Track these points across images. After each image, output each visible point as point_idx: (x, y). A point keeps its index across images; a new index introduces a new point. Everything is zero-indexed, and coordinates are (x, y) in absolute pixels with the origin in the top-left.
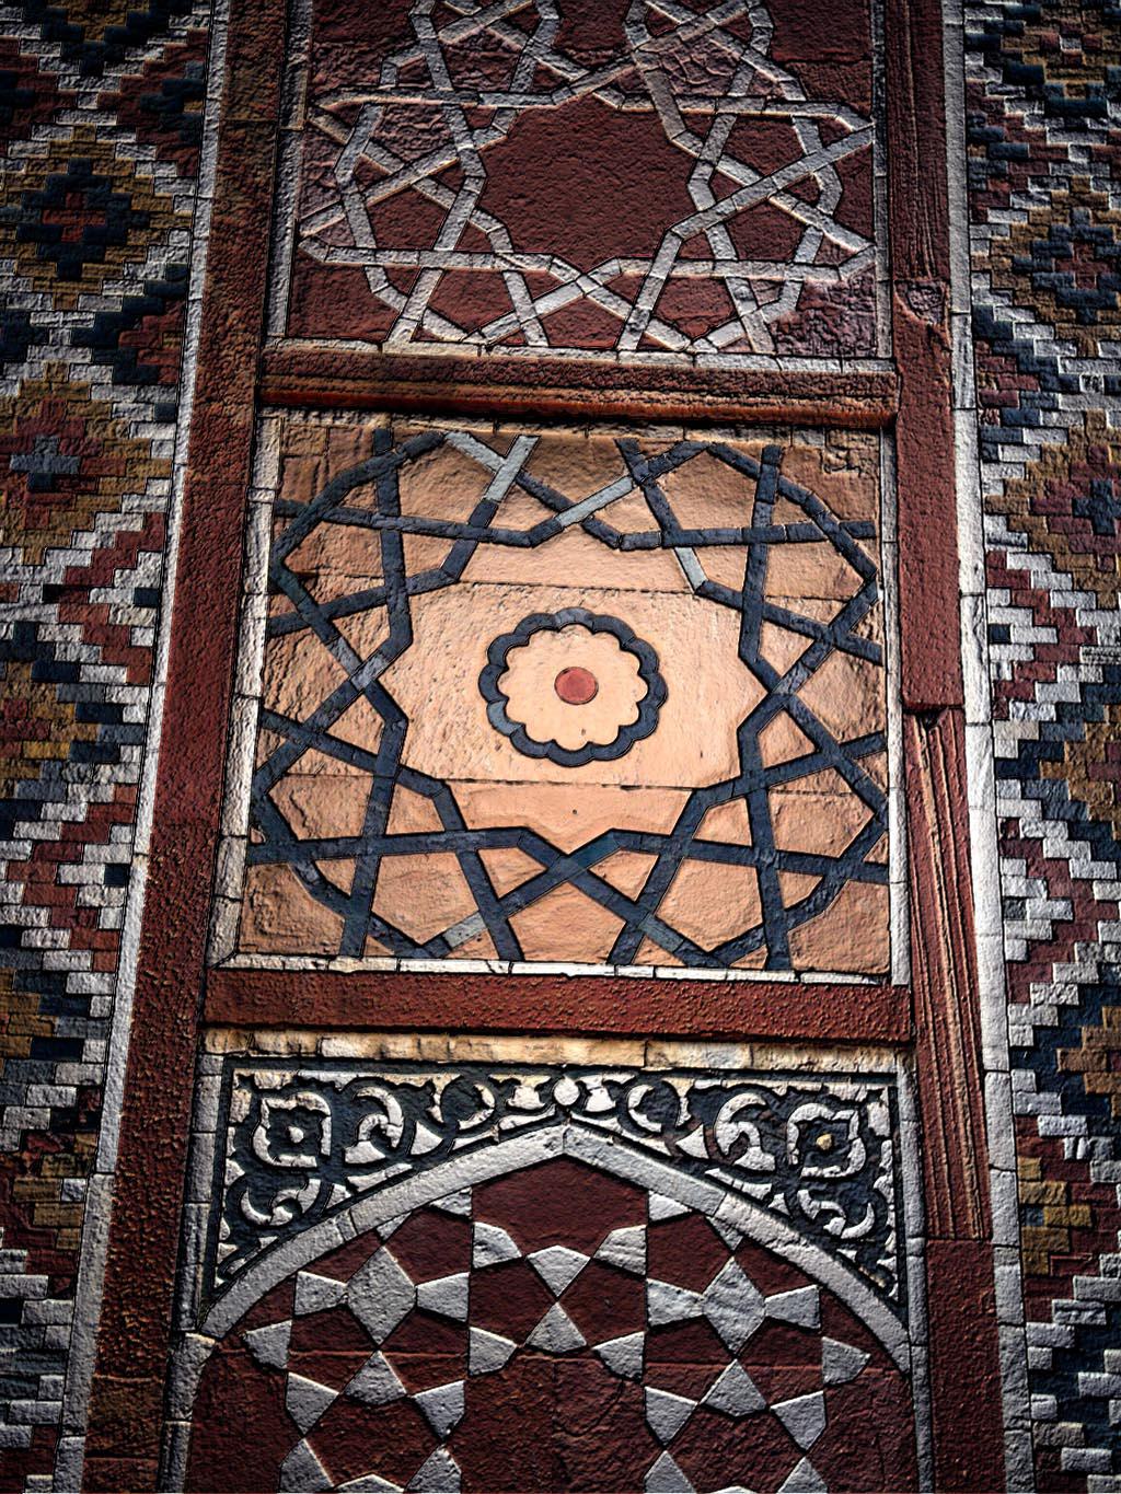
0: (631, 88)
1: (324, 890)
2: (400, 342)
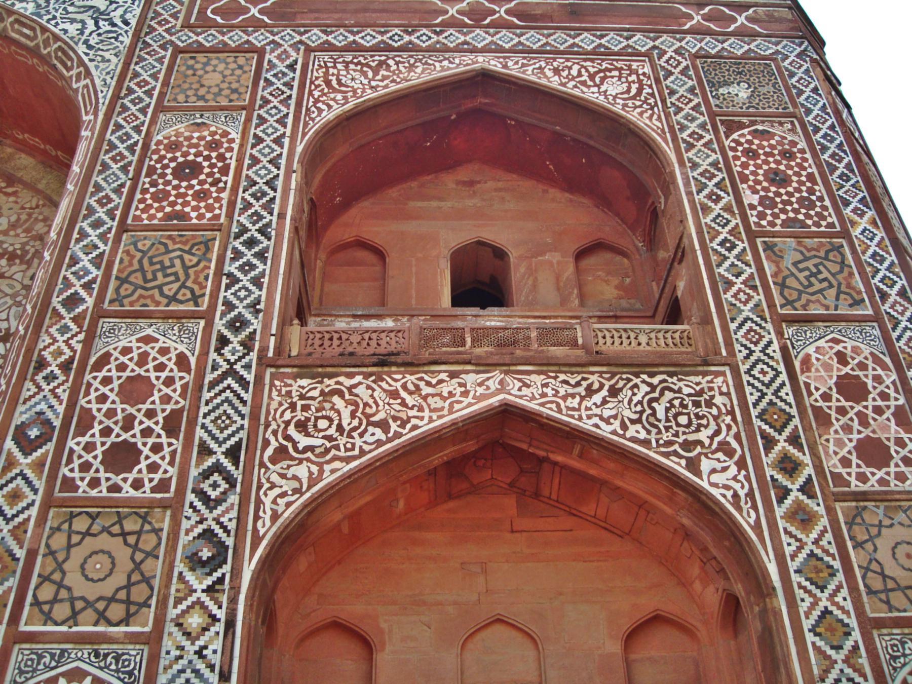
0: (874, 432)
1: (881, 600)
2: (853, 488)
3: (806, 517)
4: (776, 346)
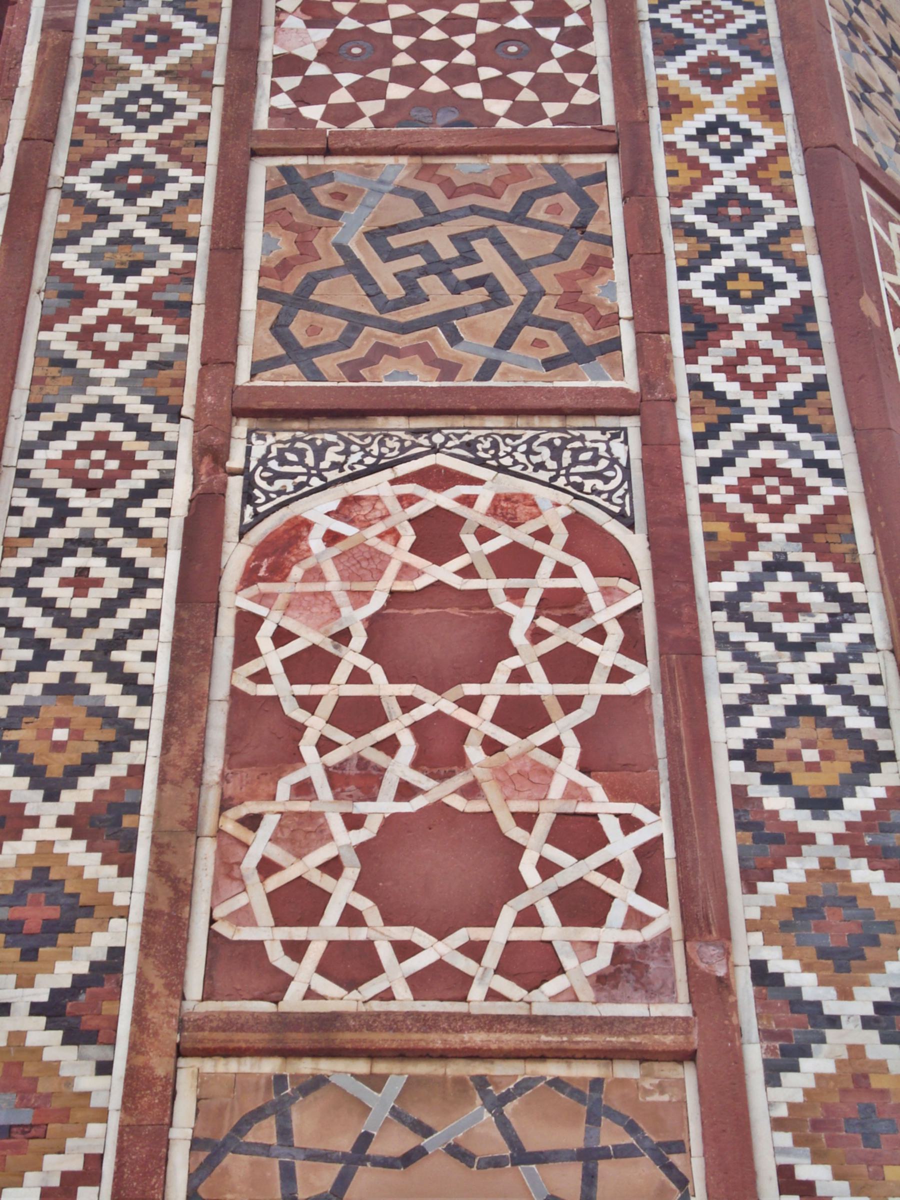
2: (293, 1001)
3: (25, 1117)
4: (179, 497)
